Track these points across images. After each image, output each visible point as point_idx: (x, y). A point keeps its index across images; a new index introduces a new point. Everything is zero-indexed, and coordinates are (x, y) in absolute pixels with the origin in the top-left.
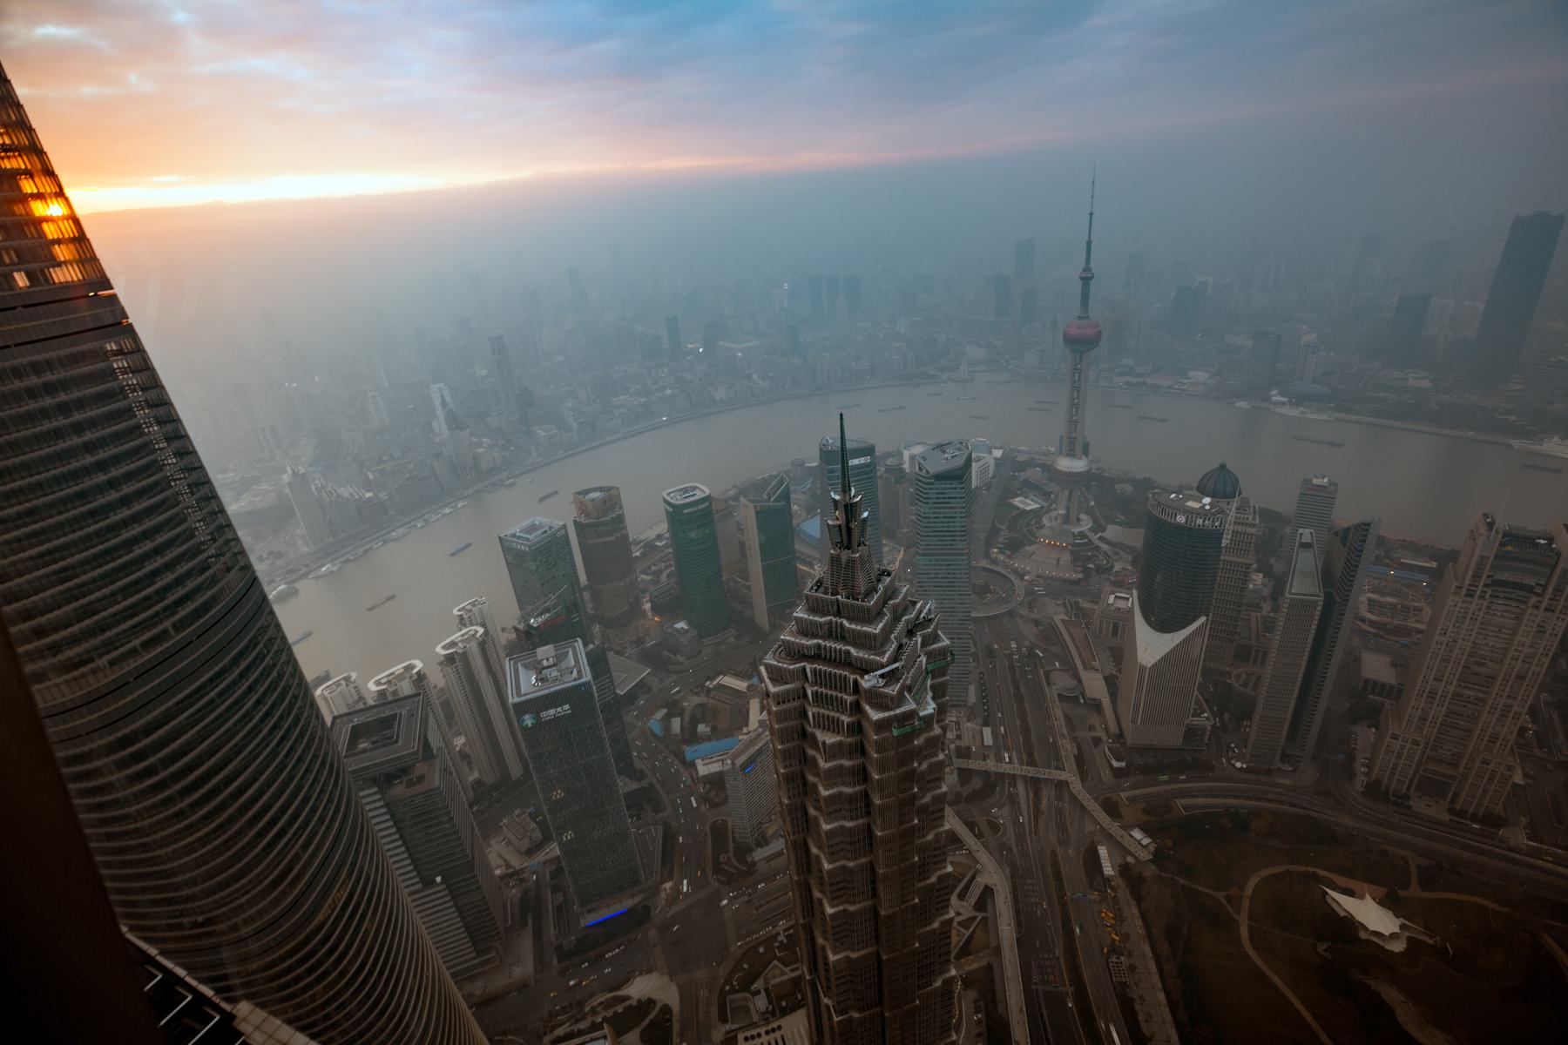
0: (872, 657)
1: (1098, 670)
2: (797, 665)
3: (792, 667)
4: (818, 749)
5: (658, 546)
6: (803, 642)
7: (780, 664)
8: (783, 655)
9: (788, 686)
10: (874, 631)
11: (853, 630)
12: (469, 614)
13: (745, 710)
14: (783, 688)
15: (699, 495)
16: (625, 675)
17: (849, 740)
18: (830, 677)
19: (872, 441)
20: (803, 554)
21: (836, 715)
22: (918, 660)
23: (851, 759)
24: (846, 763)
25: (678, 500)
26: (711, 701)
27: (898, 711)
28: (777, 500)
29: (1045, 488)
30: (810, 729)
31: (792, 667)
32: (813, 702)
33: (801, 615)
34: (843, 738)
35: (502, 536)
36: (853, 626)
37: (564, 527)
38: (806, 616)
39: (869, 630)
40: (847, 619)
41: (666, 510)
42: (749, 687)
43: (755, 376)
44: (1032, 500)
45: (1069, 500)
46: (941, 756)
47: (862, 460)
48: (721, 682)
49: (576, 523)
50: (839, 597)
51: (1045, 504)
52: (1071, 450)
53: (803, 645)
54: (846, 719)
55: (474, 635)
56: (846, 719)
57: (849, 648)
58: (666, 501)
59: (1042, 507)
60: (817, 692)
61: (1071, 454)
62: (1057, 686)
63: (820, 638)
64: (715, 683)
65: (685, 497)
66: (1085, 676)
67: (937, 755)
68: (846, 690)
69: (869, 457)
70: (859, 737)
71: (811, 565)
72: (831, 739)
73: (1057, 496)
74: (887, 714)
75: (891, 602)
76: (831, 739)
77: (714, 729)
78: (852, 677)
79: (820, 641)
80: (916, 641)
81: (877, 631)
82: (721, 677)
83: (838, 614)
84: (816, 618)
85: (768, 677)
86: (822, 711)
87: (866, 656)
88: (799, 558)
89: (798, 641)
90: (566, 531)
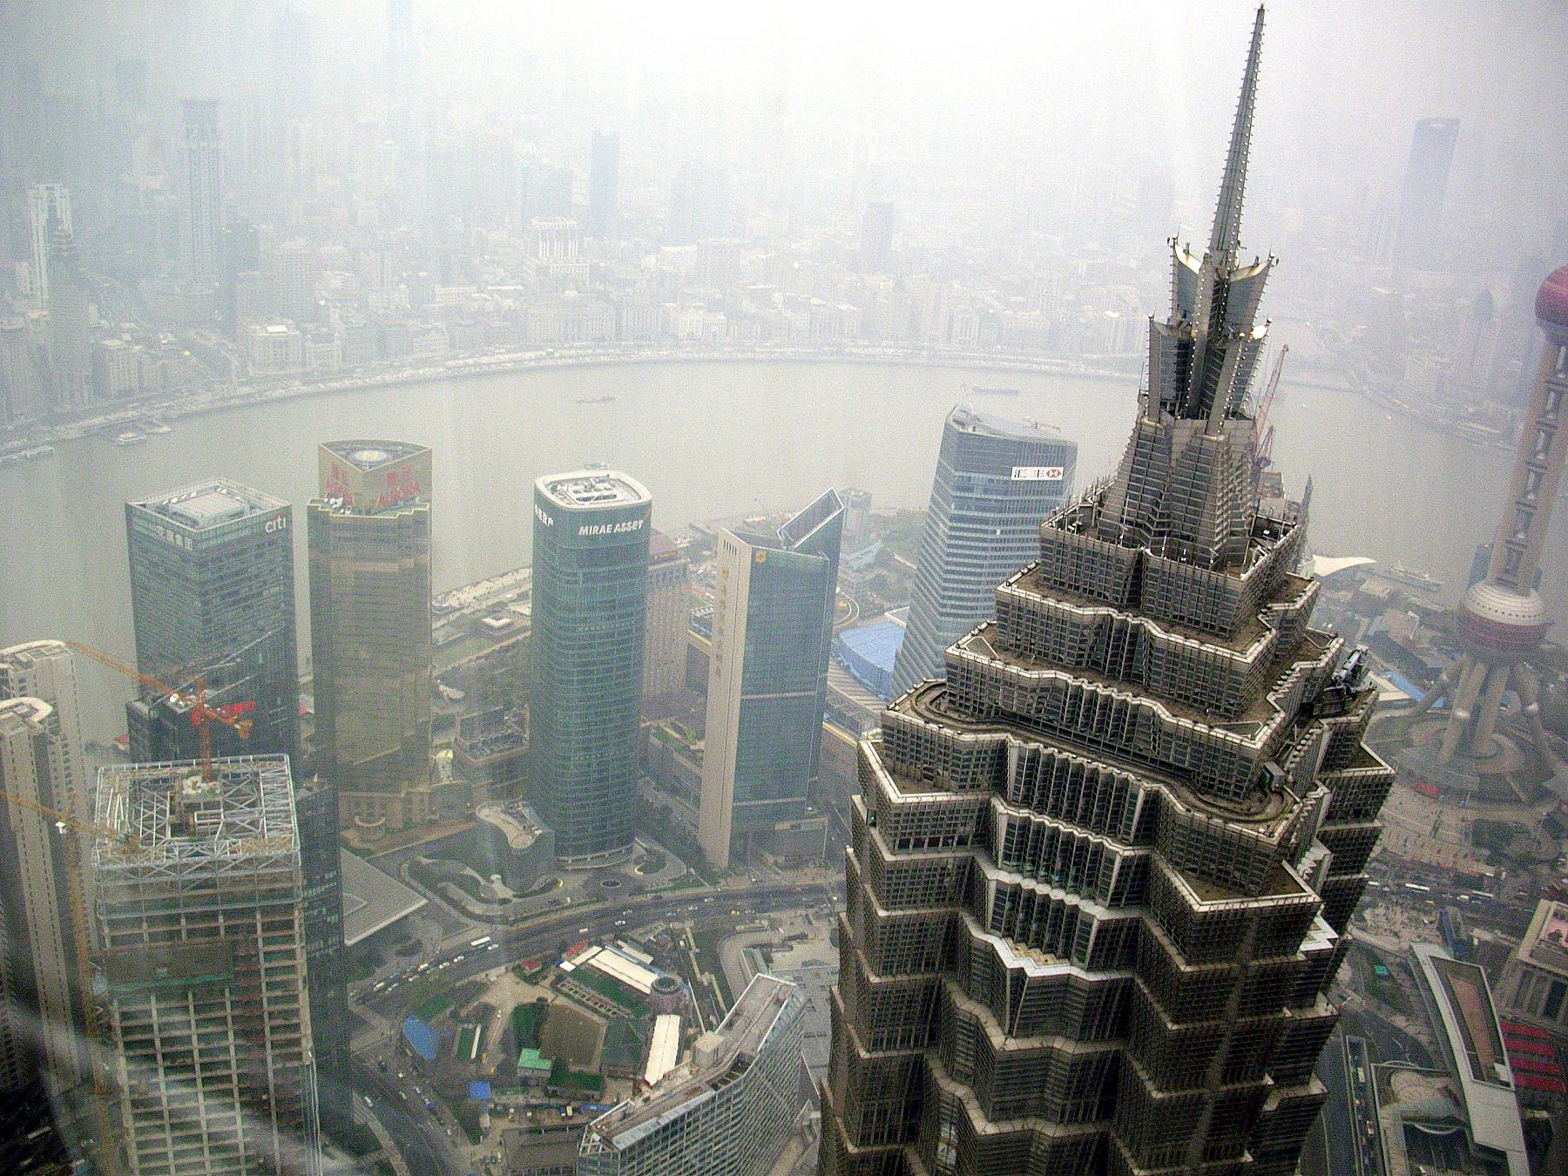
0: (1219, 733)
1: (1508, 1085)
2: (987, 737)
3: (968, 737)
4: (993, 1004)
5: (491, 628)
6: (1013, 669)
7: (934, 727)
8: (944, 704)
9: (941, 797)
10: (1237, 657)
11: (1175, 656)
12: (22, 672)
13: (641, 1037)
14: (927, 798)
15: (623, 499)
16: (365, 903)
17: (1093, 977)
18: (1076, 783)
19: (1065, 436)
20: (842, 700)
21: (1071, 900)
22: (1312, 794)
23: (1083, 1038)
24: (1066, 1047)
25: (570, 500)
26: (561, 1001)
27: (1266, 903)
28: (805, 549)
29: (1424, 659)
30: (977, 934)
31: (968, 737)
32: (1007, 857)
33: (1022, 593)
34: (1076, 971)
35: (134, 504)
36: (1176, 638)
37: (286, 513)
38: (1035, 597)
39: (1224, 652)
40: (1155, 619)
41: (536, 517)
42: (661, 982)
43: (777, 297)
44: (1390, 680)
45: (1483, 691)
46: (1316, 1088)
47: (1044, 473)
48: (592, 962)
49: (315, 517)
50: (1148, 551)
51: (1420, 696)
52: (1507, 571)
53: (1010, 683)
54: (1098, 912)
55: (24, 716)
56: (1098, 912)
57: (1146, 702)
58: (541, 500)
59: (1411, 703)
60: (1026, 824)
61: (1508, 580)
62: (1403, 1106)
63: (1064, 668)
64: (579, 960)
65: (585, 499)
66: (1476, 1093)
67: (1305, 1083)
68: (1113, 827)
69: (1061, 469)
70: (1126, 975)
71: (855, 728)
72: (1037, 966)
73: (1455, 677)
74: (1235, 904)
75: (1277, 607)
76: (1037, 966)
77: (558, 1070)
78: (1146, 785)
79: (1064, 676)
80: (1321, 735)
81: (1250, 660)
82: (596, 949)
83: (1134, 599)
84: (1066, 606)
85: (885, 767)
86: (1028, 884)
87: (1202, 728)
88: (829, 707)
89: (999, 665)
90: (290, 522)
